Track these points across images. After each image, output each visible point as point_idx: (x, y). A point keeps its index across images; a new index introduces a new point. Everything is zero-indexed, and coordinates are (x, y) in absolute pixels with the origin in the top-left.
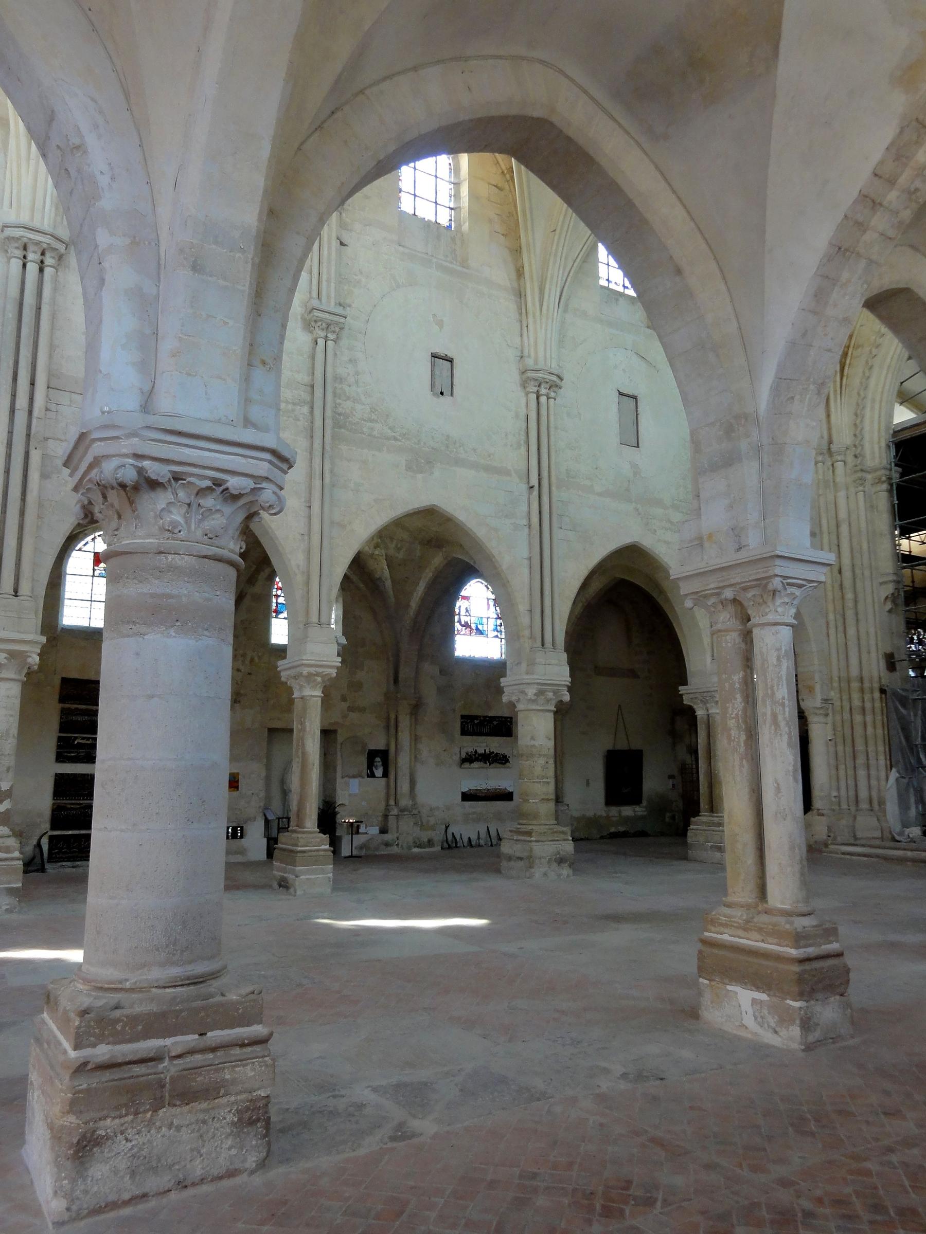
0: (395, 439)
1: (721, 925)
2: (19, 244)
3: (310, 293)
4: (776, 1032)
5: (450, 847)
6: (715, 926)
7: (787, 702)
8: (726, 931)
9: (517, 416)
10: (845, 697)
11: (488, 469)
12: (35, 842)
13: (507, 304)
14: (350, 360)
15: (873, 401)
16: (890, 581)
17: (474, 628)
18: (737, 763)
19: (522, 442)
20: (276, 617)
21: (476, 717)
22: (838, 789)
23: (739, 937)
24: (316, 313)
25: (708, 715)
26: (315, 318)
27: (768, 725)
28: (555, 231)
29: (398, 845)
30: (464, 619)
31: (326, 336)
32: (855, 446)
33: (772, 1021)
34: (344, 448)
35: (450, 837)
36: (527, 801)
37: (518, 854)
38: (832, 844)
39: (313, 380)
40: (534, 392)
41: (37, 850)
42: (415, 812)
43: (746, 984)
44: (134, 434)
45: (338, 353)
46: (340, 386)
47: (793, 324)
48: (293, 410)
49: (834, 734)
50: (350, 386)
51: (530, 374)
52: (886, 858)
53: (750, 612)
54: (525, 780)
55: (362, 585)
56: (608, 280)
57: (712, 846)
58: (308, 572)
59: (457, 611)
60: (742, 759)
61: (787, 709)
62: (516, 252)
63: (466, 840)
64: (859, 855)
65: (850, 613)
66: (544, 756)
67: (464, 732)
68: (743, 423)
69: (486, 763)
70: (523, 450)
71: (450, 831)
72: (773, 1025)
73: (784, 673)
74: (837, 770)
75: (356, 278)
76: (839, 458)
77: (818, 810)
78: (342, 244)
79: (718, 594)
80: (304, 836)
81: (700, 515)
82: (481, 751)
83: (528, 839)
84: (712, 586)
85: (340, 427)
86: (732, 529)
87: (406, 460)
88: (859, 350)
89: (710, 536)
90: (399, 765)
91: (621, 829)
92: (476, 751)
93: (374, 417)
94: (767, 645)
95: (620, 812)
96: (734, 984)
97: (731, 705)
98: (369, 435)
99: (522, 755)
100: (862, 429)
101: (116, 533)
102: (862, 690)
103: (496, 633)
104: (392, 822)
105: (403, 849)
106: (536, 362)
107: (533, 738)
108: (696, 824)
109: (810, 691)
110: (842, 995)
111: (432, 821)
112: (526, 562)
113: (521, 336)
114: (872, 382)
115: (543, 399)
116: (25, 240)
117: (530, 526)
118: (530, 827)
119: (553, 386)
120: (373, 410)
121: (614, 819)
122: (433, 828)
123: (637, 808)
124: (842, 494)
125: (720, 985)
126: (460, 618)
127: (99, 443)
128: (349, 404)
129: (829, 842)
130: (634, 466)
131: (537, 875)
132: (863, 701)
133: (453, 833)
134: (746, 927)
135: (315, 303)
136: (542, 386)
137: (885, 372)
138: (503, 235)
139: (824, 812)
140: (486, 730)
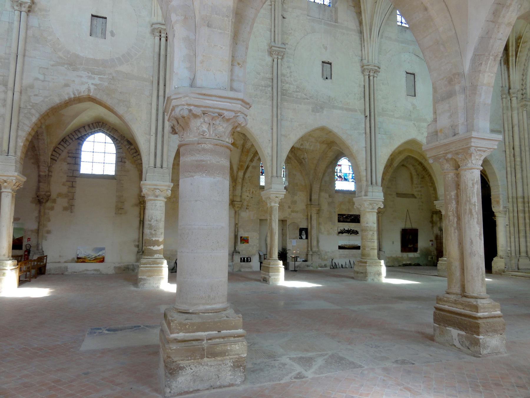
0: (307, 99)
1: (444, 301)
2: (158, 31)
3: (271, 40)
4: (469, 349)
5: (333, 268)
6: (442, 302)
7: (476, 204)
8: (446, 304)
9: (360, 86)
10: (515, 205)
11: (347, 109)
12: (174, 261)
13: (355, 37)
14: (288, 67)
17: (343, 178)
18: (453, 231)
19: (362, 97)
20: (262, 175)
21: (344, 215)
22: (511, 247)
23: (453, 307)
24: (273, 48)
26: (273, 50)
27: (467, 214)
28: (376, 2)
29: (312, 266)
30: (339, 174)
31: (278, 58)
32: (522, 90)
33: (467, 343)
34: (285, 104)
35: (334, 264)
37: (361, 271)
38: (507, 271)
39: (273, 76)
40: (367, 75)
41: (175, 264)
42: (319, 253)
43: (455, 327)
44: (186, 96)
45: (283, 64)
46: (284, 78)
47: (482, 28)
48: (265, 90)
49: (509, 222)
50: (288, 78)
53: (459, 163)
55: (296, 161)
56: (401, 22)
58: (272, 155)
59: (336, 171)
60: (455, 230)
61: (477, 207)
62: (359, 13)
63: (340, 265)
65: (518, 167)
66: (372, 230)
67: (339, 221)
68: (457, 77)
69: (348, 234)
70: (363, 100)
71: (333, 261)
72: (467, 345)
73: (475, 191)
74: (510, 238)
75: (290, 32)
76: (514, 95)
78: (284, 18)
79: (445, 156)
80: (272, 261)
81: (436, 121)
82: (346, 229)
83: (366, 265)
84: (441, 153)
85: (284, 95)
86: (451, 127)
87: (312, 108)
88: (525, 44)
89: (441, 130)
90: (312, 234)
91: (408, 262)
92: (344, 229)
93: (298, 90)
94: (467, 178)
95: (408, 255)
96: (450, 326)
97: (450, 206)
98: (296, 98)
100: (526, 81)
101: (183, 136)
102: (524, 203)
103: (353, 180)
104: (310, 258)
105: (314, 268)
106: (368, 62)
107: (367, 223)
108: (442, 261)
109: (497, 203)
110: (501, 334)
111: (326, 257)
112: (364, 149)
113: (362, 50)
115: (371, 78)
116: (160, 29)
117: (366, 133)
118: (366, 260)
119: (376, 72)
120: (298, 87)
121: (405, 258)
122: (326, 260)
123: (415, 254)
125: (444, 327)
126: (337, 174)
127: (174, 100)
128: (288, 85)
129: (505, 270)
130: (413, 105)
131: (369, 280)
132: (524, 207)
133: (335, 262)
134: (455, 302)
135: (273, 44)
136: (371, 72)
138: (353, 7)
139: (503, 257)
140: (349, 220)
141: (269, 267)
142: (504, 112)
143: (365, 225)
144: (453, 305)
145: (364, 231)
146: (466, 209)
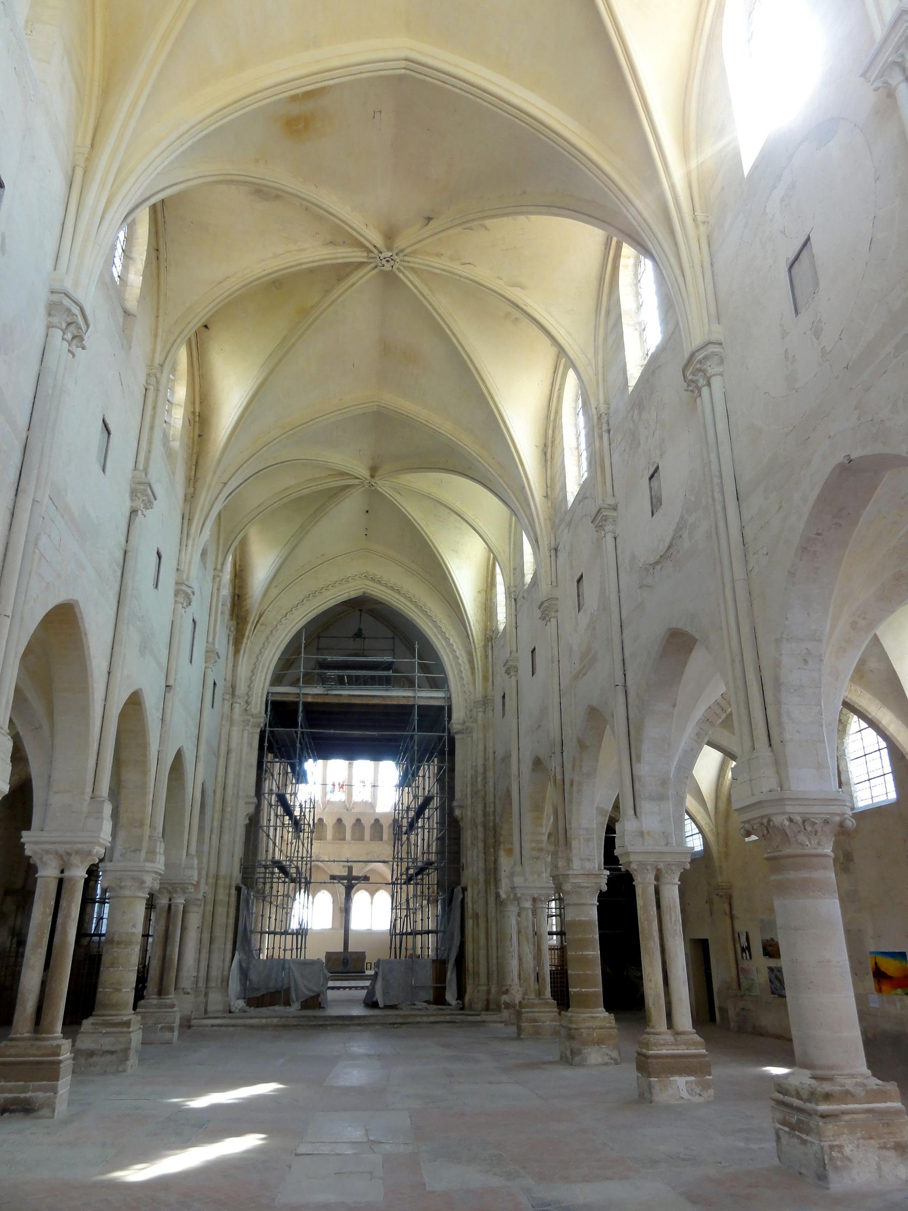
15: (263, 666)
16: (253, 803)
25: (170, 906)
28: (225, 484)
32: (247, 694)
36: (119, 990)
37: (106, 1048)
38: (194, 1019)
43: (681, 1074)
51: (184, 588)
52: (252, 1027)
54: (121, 968)
57: (162, 1028)
64: (228, 1026)
65: (226, 823)
76: (238, 700)
77: (183, 989)
84: (652, 860)
89: (648, 833)
99: (119, 943)
106: (188, 579)
113: (180, 550)
114: (267, 652)
124: (235, 729)
125: (665, 1079)
137: (275, 649)
139: (189, 991)
141: (60, 1062)
142: (224, 722)
143: (130, 931)
144: (673, 1047)
145: (123, 946)
146: (676, 930)
